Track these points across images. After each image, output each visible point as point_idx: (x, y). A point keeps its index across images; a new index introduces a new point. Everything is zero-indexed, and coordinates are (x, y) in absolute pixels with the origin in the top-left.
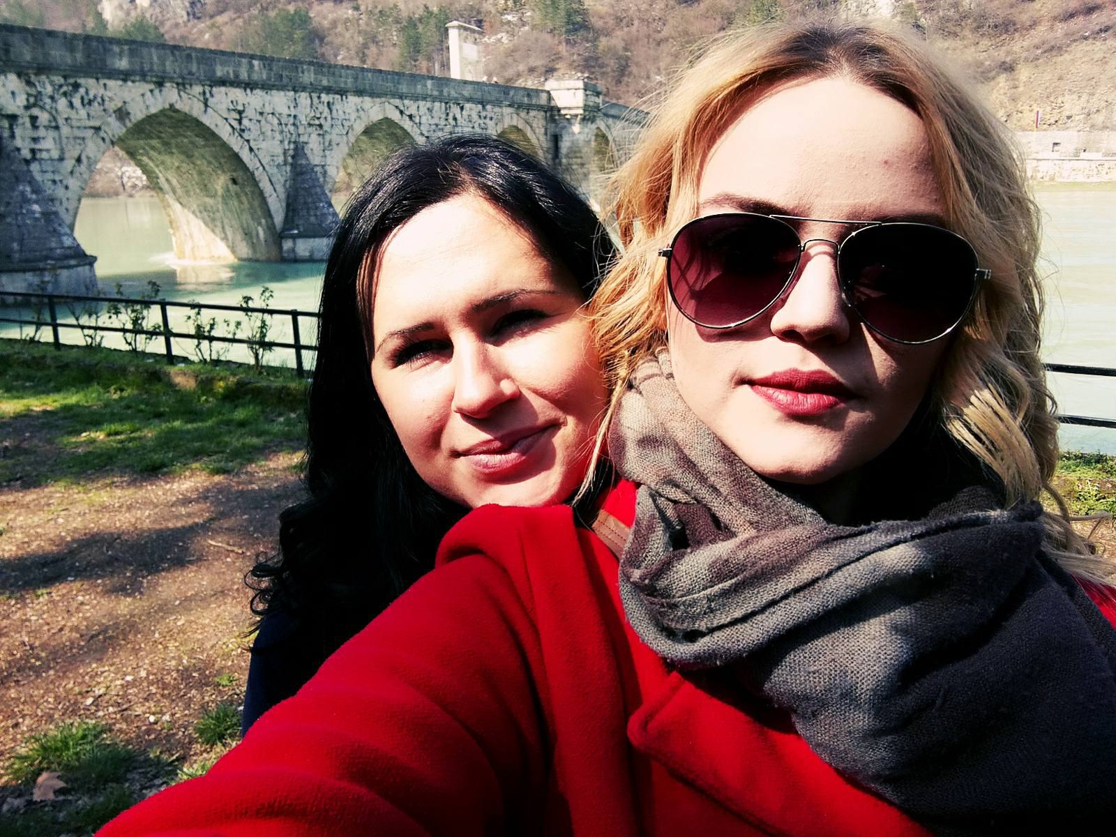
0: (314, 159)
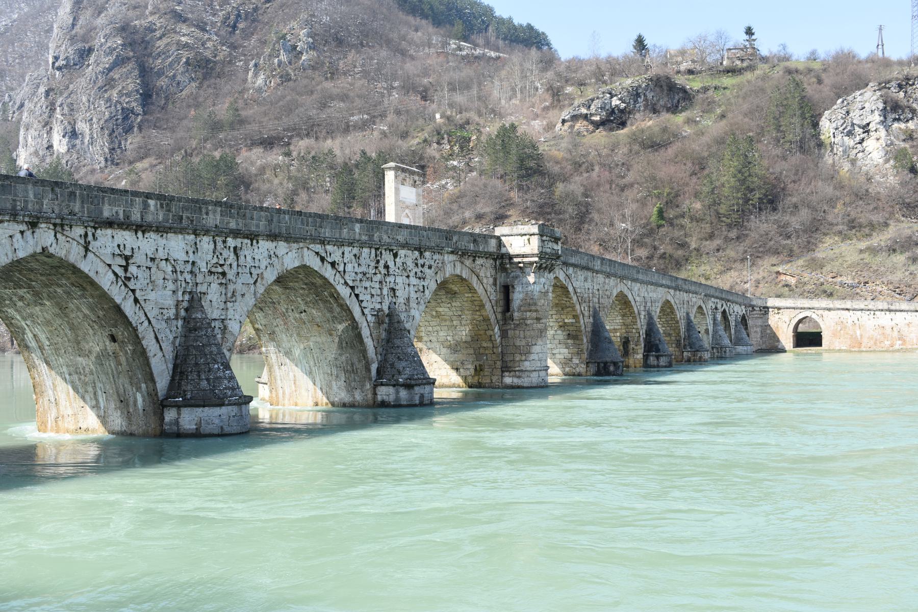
0: (212, 312)
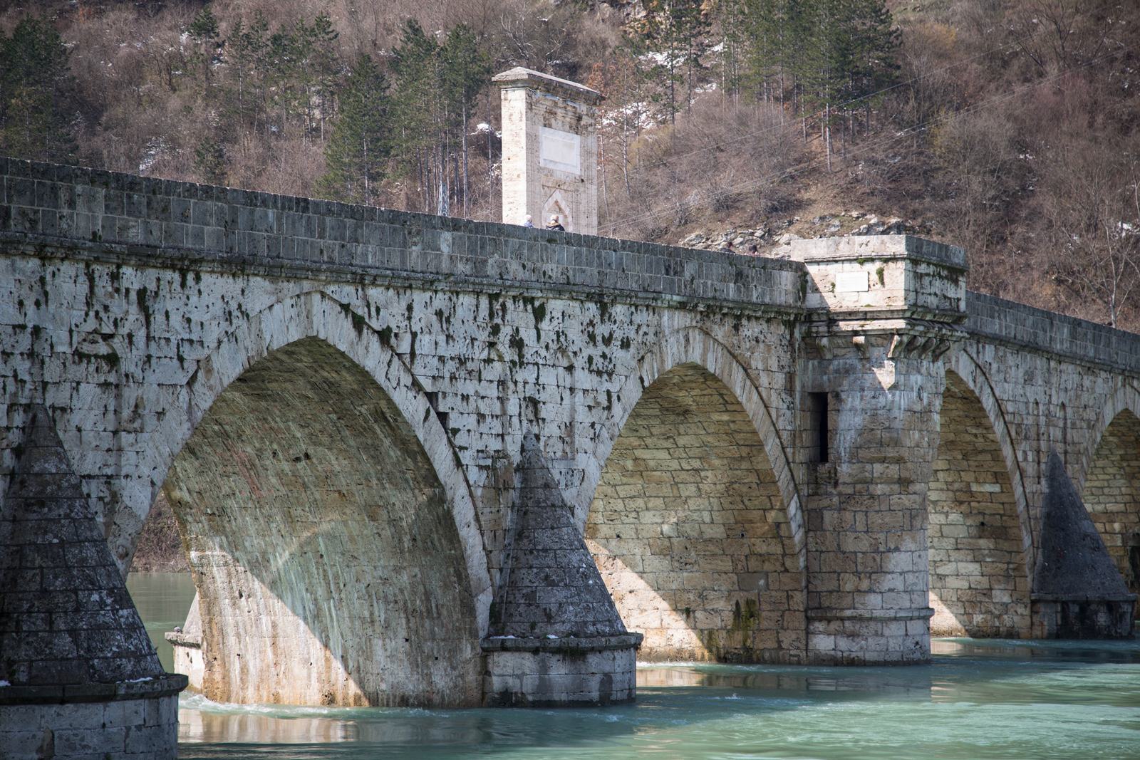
0: (83, 457)
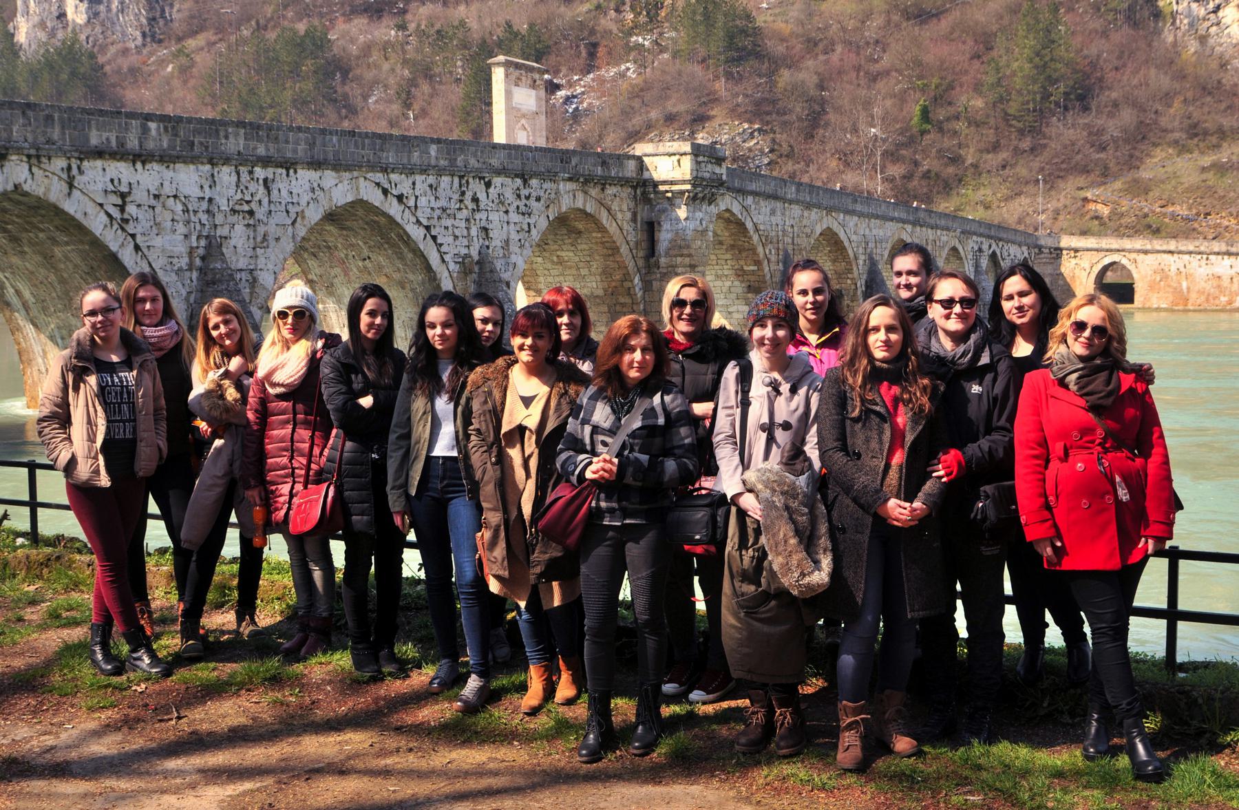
0: (237, 261)
